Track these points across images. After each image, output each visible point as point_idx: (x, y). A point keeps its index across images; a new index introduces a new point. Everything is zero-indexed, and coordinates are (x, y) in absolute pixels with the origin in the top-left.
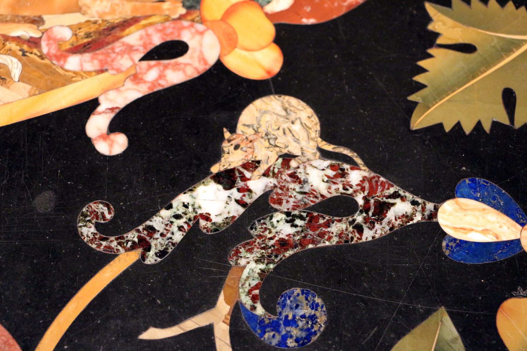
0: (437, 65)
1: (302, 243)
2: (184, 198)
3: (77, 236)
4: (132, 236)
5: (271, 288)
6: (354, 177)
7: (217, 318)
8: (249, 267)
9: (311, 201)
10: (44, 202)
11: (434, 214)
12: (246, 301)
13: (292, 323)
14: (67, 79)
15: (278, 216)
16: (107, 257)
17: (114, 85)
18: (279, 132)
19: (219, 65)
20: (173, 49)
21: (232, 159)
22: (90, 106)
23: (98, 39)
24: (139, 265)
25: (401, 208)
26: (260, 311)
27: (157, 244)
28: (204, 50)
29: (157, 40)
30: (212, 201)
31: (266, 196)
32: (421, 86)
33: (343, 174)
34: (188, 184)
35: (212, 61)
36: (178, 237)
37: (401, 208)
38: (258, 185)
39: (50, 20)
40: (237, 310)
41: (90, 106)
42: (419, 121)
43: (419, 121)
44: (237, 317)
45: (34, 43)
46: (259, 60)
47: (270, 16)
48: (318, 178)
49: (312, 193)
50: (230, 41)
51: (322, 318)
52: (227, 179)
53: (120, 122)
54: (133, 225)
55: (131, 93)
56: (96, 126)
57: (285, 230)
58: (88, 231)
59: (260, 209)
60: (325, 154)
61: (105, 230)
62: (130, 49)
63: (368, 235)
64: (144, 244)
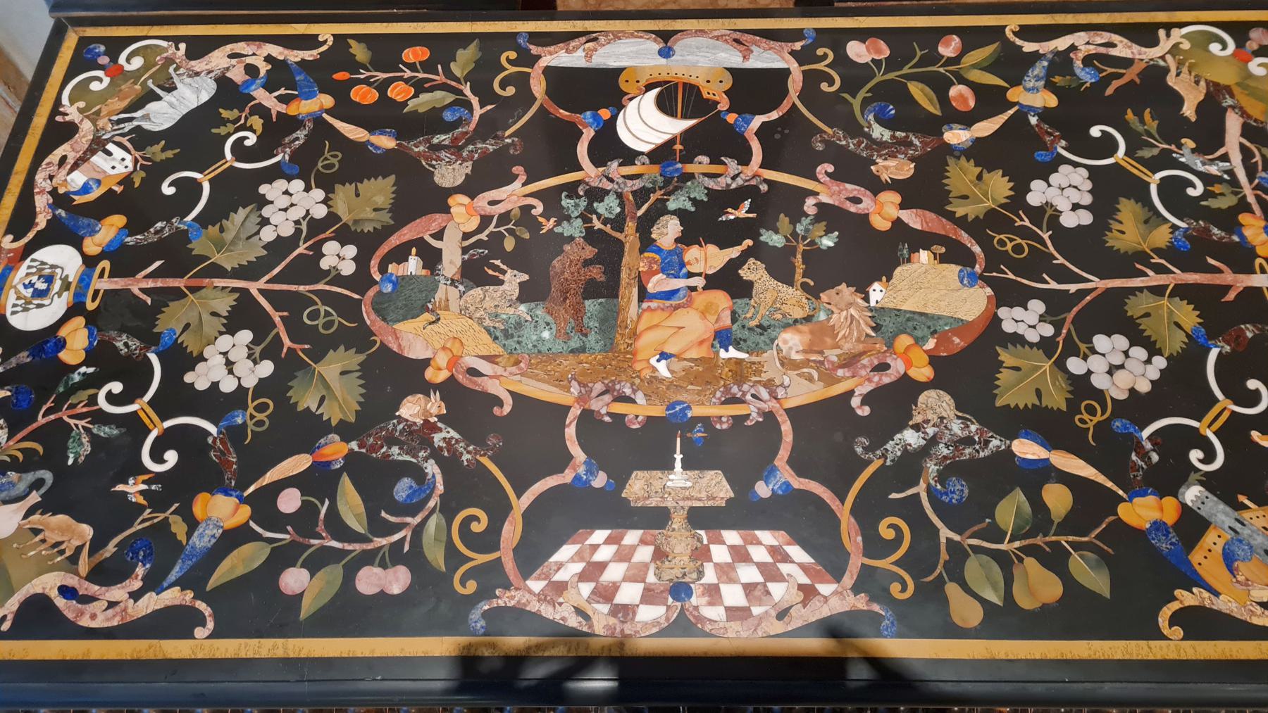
0: (1004, 377)
1: (954, 457)
2: (898, 436)
3: (855, 452)
4: (879, 452)
5: (942, 477)
6: (973, 428)
7: (921, 489)
8: (932, 468)
9: (955, 439)
10: (838, 437)
11: (1010, 446)
12: (932, 482)
13: (953, 492)
14: (839, 380)
15: (941, 445)
16: (869, 462)
17: (859, 385)
18: (936, 405)
19: (905, 374)
20: (883, 367)
21: (918, 419)
22: (851, 393)
23: (850, 361)
24: (883, 465)
25: (995, 443)
26: (939, 487)
27: (890, 456)
28: (898, 368)
29: (876, 362)
30: (911, 438)
31: (935, 436)
32: (998, 387)
33: (968, 426)
34: (900, 429)
35: (902, 372)
36: (899, 454)
37: (995, 443)
38: (931, 431)
39: (827, 352)
40: (929, 486)
41: (851, 393)
42: (999, 403)
43: (999, 403)
44: (929, 489)
45: (821, 363)
46: (923, 372)
47: (925, 352)
48: (956, 427)
49: (955, 435)
50: (909, 364)
51: (966, 491)
52: (917, 428)
53: (866, 400)
54: (879, 448)
55: (868, 388)
56: (855, 402)
57: (946, 452)
58: (859, 450)
59: (933, 441)
60: (959, 418)
61: (867, 449)
62: (864, 366)
63: (982, 454)
64: (884, 456)
